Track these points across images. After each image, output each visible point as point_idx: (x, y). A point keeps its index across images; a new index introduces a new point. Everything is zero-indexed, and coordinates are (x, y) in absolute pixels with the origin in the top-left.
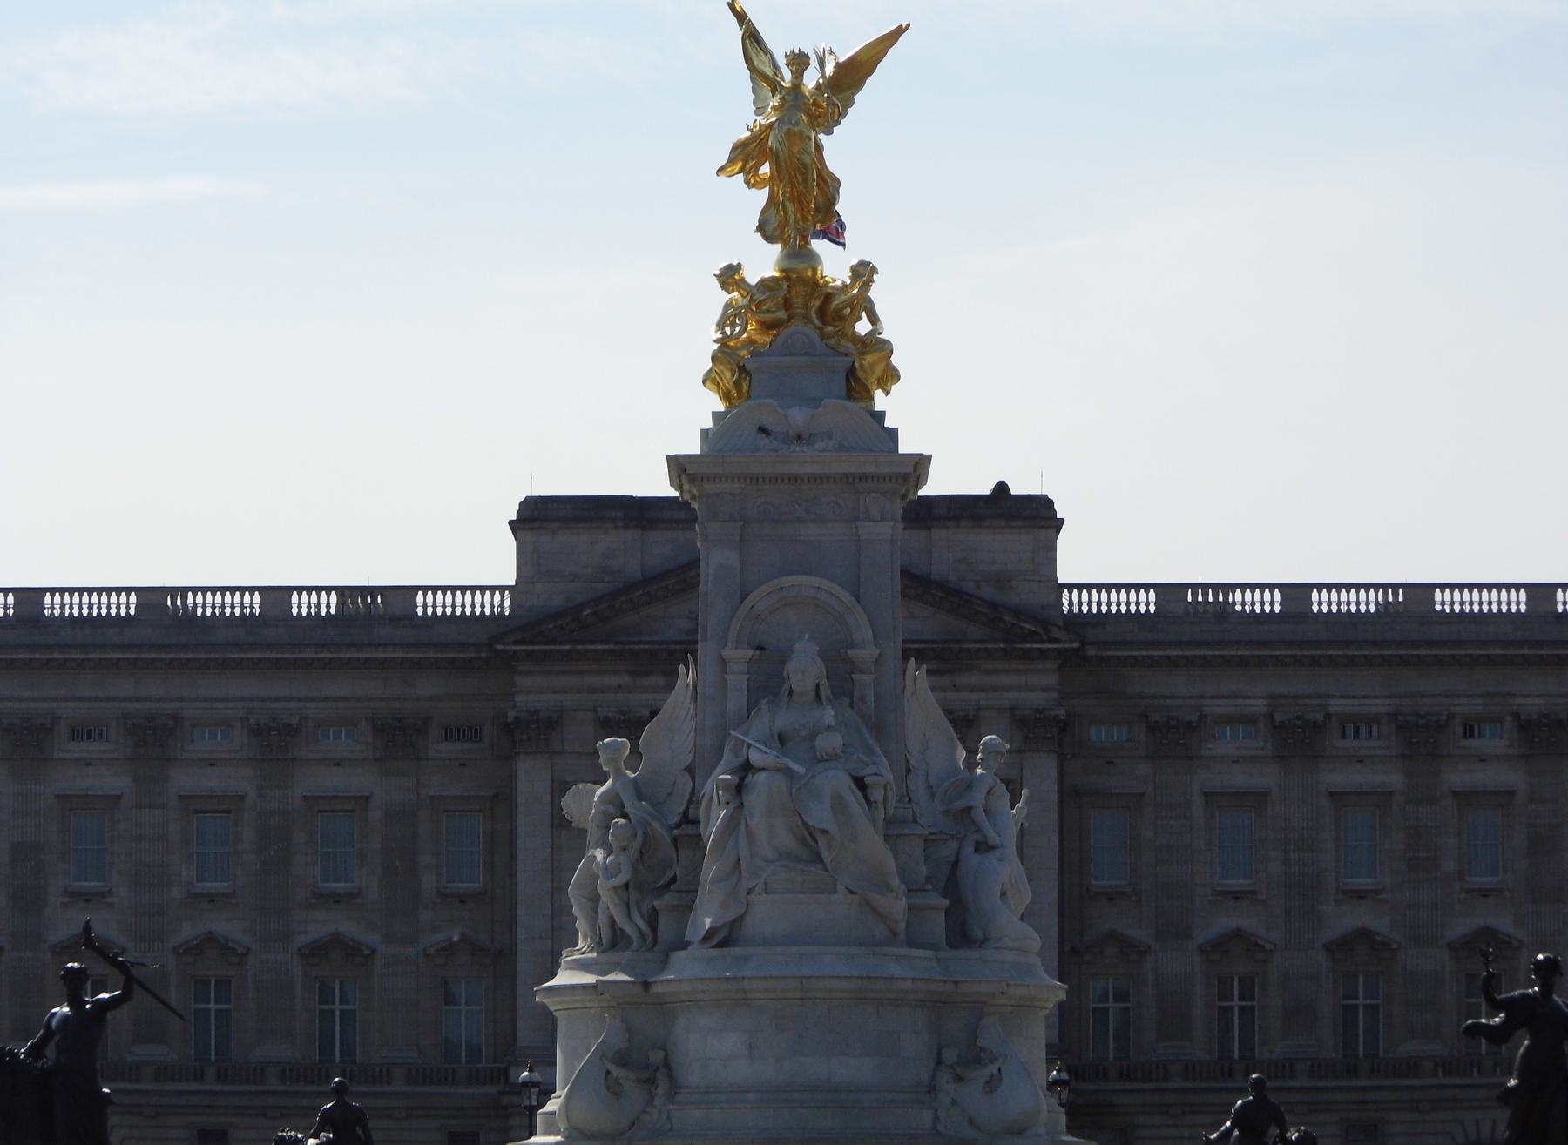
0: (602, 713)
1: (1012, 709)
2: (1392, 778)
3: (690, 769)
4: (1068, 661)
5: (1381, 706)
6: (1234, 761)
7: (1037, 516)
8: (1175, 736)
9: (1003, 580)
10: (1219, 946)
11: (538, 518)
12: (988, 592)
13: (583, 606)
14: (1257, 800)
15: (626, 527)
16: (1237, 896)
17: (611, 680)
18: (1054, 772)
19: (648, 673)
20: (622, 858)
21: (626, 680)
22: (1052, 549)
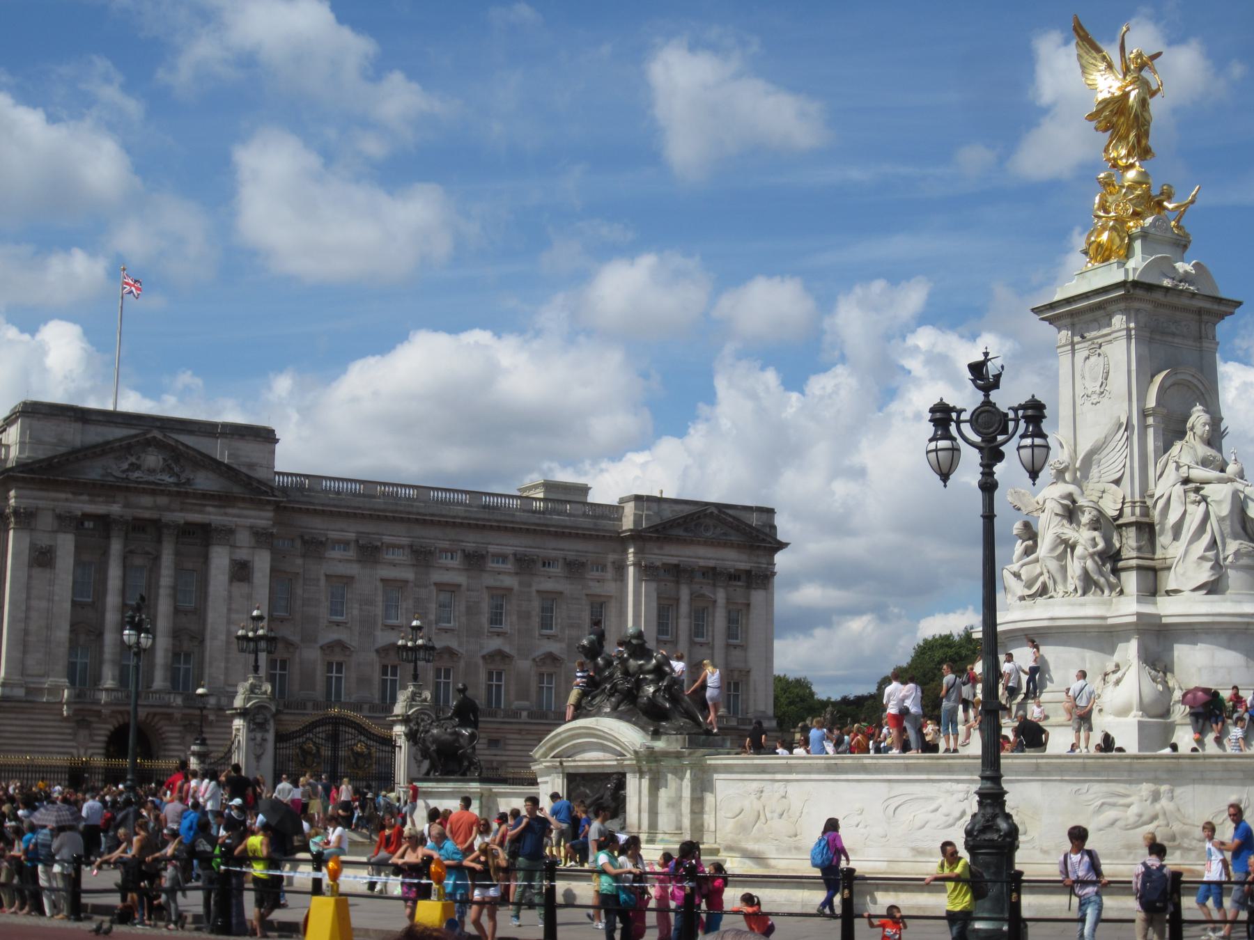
0: (57, 511)
1: (251, 527)
2: (408, 574)
3: (1117, 482)
4: (278, 507)
5: (405, 541)
6: (339, 562)
7: (267, 437)
8: (314, 547)
9: (251, 466)
10: (329, 648)
11: (31, 412)
12: (244, 470)
13: (55, 457)
14: (349, 580)
15: (76, 421)
16: (338, 624)
17: (63, 496)
18: (268, 559)
19: (81, 494)
20: (1096, 534)
21: (70, 496)
22: (273, 452)
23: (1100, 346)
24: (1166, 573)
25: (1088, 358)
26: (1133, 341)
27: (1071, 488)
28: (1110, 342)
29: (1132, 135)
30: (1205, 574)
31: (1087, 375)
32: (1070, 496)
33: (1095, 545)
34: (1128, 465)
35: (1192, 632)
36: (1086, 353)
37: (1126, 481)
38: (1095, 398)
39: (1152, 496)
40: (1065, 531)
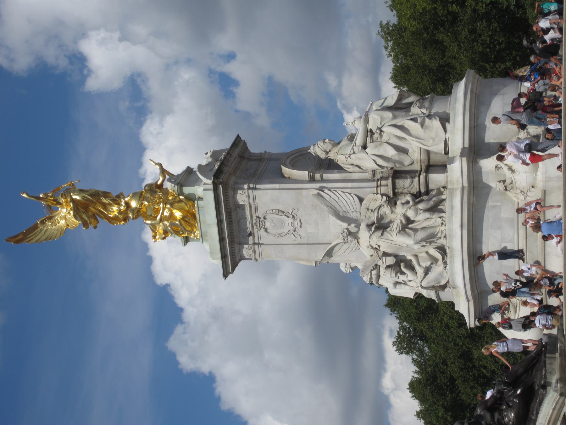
3: (361, 200)
23: (258, 217)
24: (432, 156)
25: (266, 230)
26: (258, 186)
27: (363, 226)
28: (256, 208)
29: (105, 201)
30: (436, 123)
31: (279, 231)
32: (369, 226)
33: (408, 202)
34: (349, 191)
35: (476, 129)
36: (263, 231)
37: (361, 193)
38: (297, 224)
39: (374, 172)
40: (395, 226)
